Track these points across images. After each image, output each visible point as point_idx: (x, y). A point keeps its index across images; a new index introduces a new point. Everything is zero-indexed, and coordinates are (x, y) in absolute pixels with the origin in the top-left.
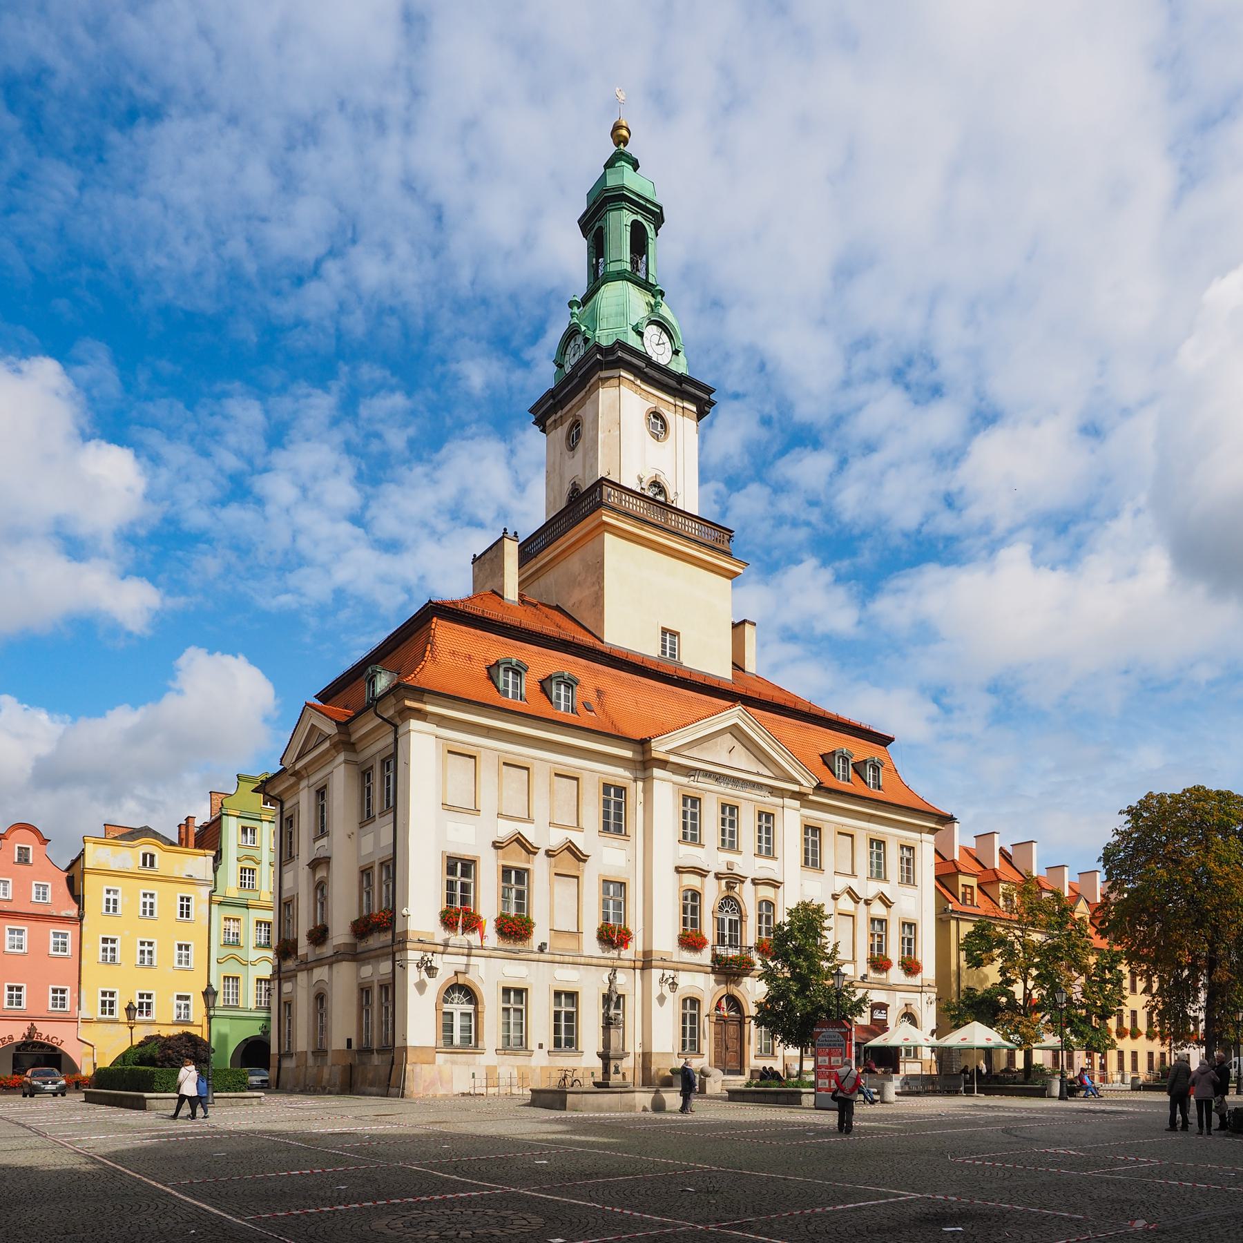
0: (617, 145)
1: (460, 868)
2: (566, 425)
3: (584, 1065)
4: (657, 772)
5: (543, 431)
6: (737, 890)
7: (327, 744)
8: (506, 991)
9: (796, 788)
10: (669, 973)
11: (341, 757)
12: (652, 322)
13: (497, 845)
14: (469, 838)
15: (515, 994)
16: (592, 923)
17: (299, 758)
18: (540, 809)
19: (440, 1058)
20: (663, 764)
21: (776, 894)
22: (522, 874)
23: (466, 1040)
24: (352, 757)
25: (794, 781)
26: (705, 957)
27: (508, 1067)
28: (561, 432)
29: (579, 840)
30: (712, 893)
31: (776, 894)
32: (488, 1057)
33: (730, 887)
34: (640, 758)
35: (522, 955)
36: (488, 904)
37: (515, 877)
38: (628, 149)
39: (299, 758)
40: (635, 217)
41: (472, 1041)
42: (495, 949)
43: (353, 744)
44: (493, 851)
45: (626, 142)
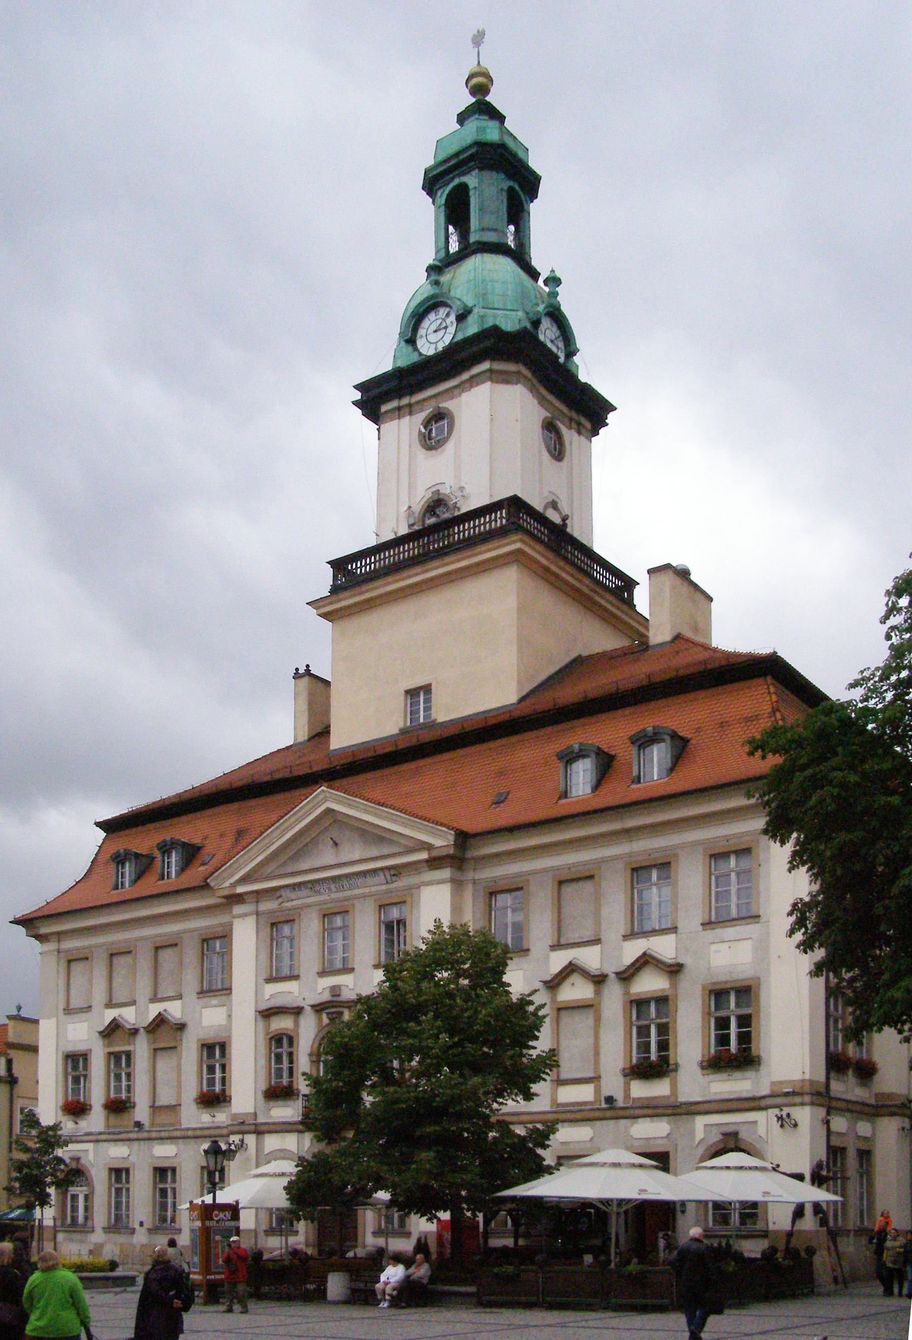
9: (424, 856)
15: (119, 1174)
25: (429, 847)
29: (174, 1010)
30: (308, 1033)
35: (123, 1136)
36: (97, 1092)
37: (120, 1062)
42: (100, 1133)
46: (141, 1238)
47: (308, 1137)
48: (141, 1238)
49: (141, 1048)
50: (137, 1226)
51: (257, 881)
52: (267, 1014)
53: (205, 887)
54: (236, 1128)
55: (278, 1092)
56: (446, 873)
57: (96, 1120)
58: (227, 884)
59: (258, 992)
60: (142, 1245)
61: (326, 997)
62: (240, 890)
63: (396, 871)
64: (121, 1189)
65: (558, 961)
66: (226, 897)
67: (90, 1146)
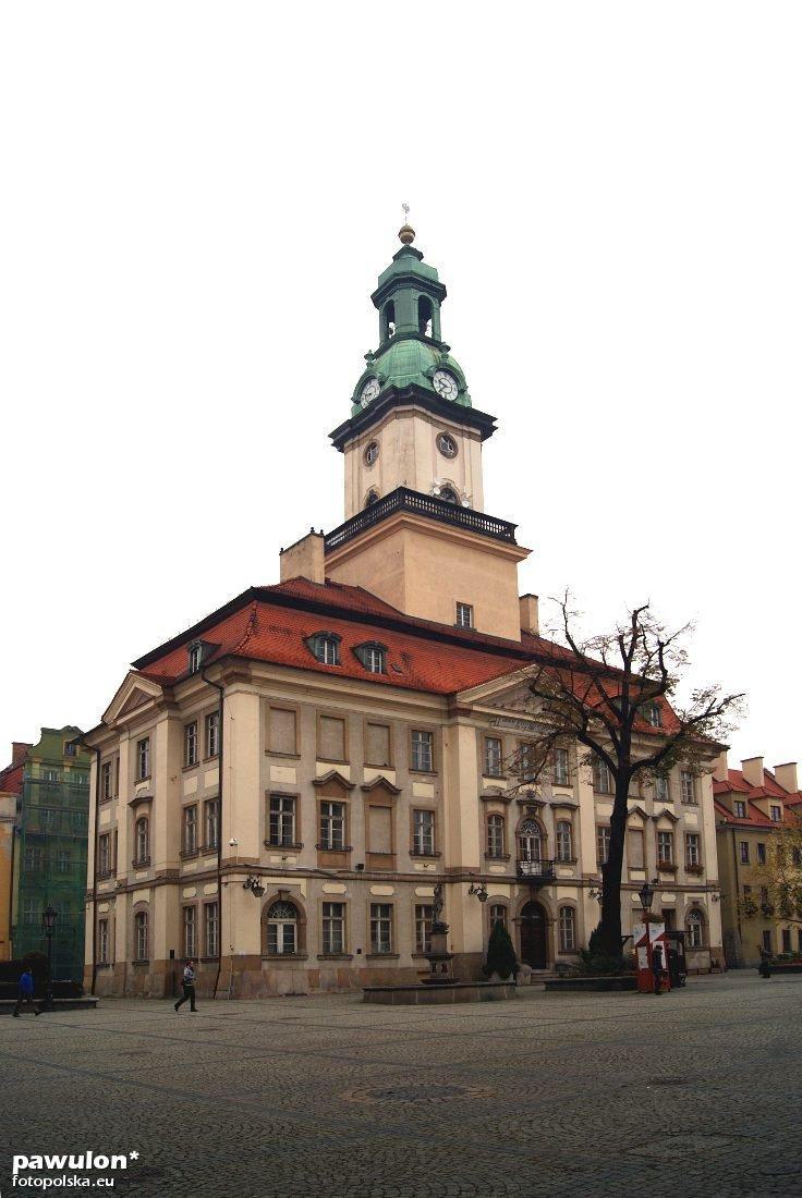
0: (403, 240)
1: (280, 804)
2: (363, 447)
3: (400, 966)
4: (461, 719)
5: (341, 450)
6: (537, 813)
7: (151, 704)
8: (326, 906)
10: (477, 886)
11: (165, 715)
12: (439, 370)
13: (317, 784)
16: (403, 843)
17: (121, 715)
18: (355, 751)
19: (266, 965)
20: (467, 712)
21: (573, 817)
23: (289, 948)
24: (175, 714)
27: (330, 970)
28: (358, 452)
29: (390, 776)
30: (513, 817)
32: (312, 963)
33: (531, 811)
34: (444, 708)
38: (412, 245)
39: (121, 715)
40: (421, 293)
41: (294, 952)
42: (316, 871)
43: (177, 703)
44: (312, 790)
45: (411, 240)
46: (359, 963)
47: (517, 888)
48: (359, 963)
49: (356, 803)
50: (354, 953)
51: (494, 706)
54: (469, 878)
57: (308, 858)
58: (467, 700)
59: (480, 784)
60: (361, 970)
61: (524, 797)
62: (475, 708)
64: (329, 921)
67: (303, 882)
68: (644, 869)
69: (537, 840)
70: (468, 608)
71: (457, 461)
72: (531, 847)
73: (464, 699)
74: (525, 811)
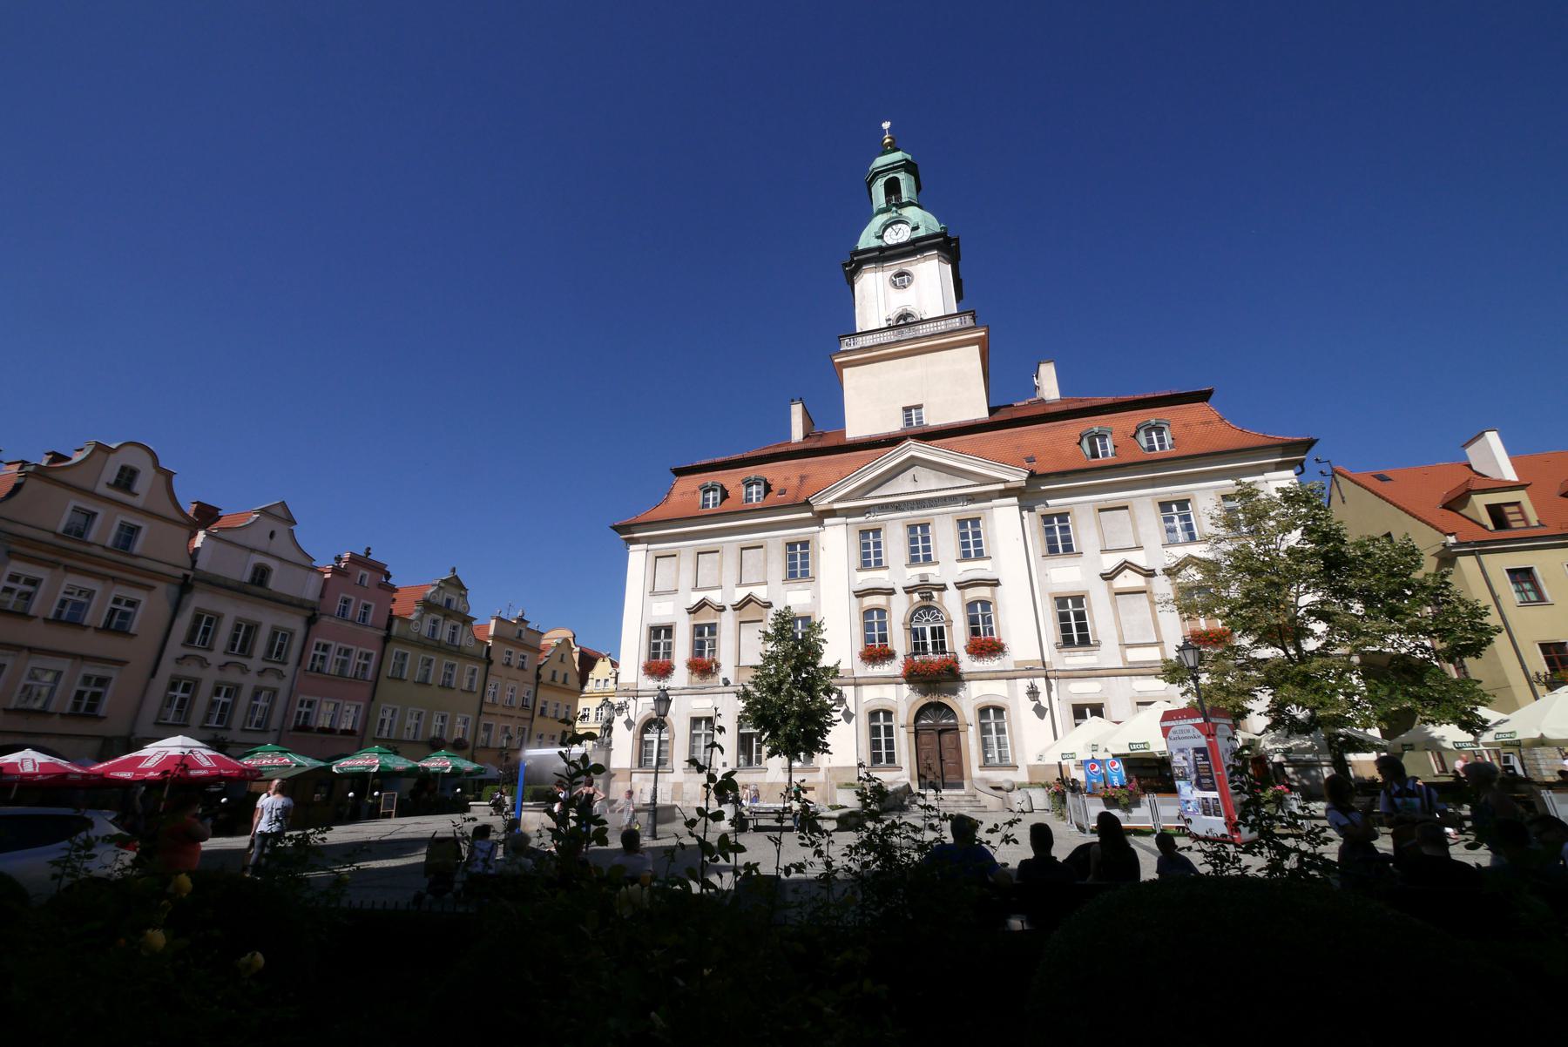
1: (660, 633)
9: (1001, 486)
14: (666, 611)
20: (832, 513)
22: (713, 628)
26: (895, 668)
29: (761, 593)
30: (899, 608)
31: (993, 593)
52: (860, 594)
53: (807, 505)
55: (876, 653)
56: (1015, 500)
61: (916, 581)
62: (836, 506)
63: (971, 498)
65: (1110, 562)
66: (822, 512)
68: (1159, 643)
69: (941, 629)
70: (919, 407)
71: (912, 288)
72: (934, 636)
73: (822, 504)
74: (916, 597)
